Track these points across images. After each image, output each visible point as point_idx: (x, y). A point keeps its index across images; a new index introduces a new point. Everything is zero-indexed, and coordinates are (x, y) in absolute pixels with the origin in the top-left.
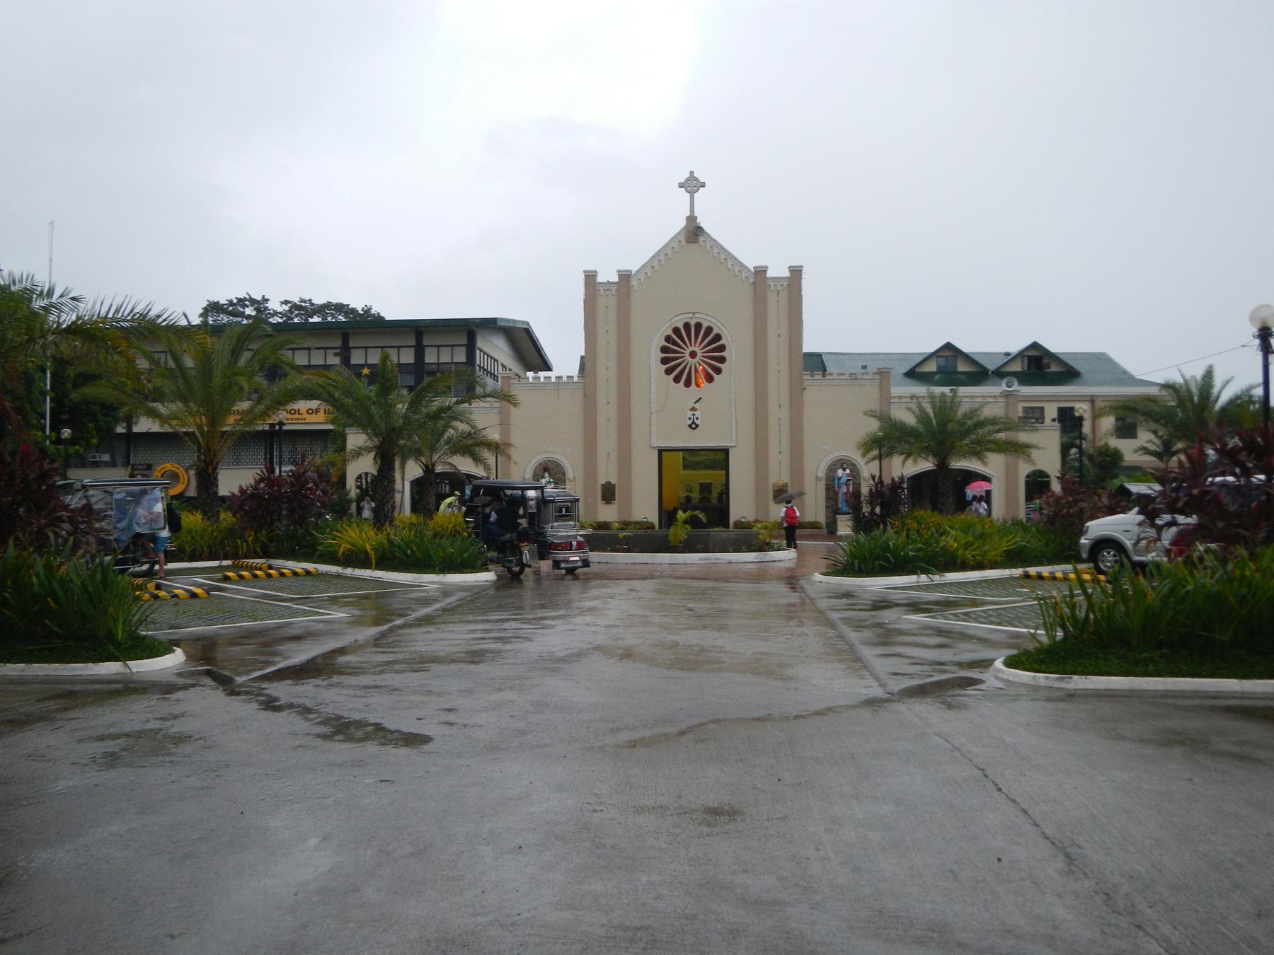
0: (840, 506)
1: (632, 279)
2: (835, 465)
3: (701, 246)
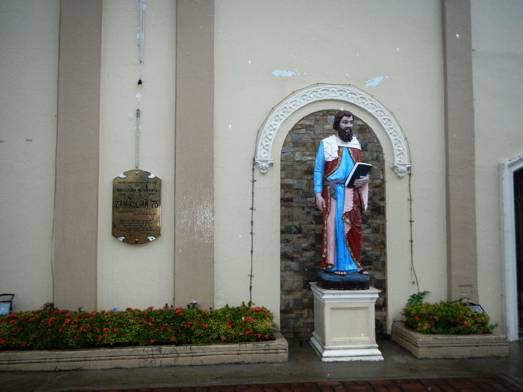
0: (331, 260)
2: (308, 127)
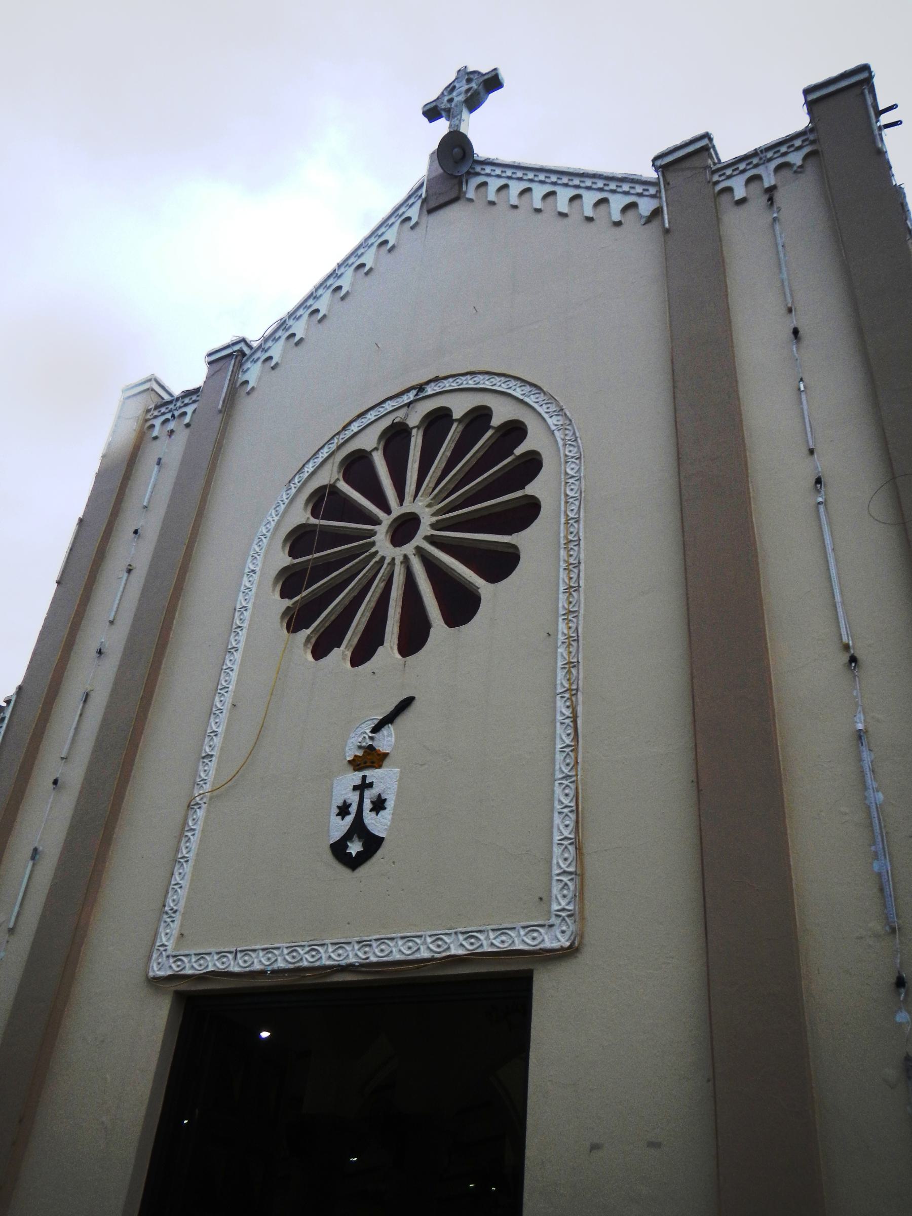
1: (248, 365)
3: (471, 200)
